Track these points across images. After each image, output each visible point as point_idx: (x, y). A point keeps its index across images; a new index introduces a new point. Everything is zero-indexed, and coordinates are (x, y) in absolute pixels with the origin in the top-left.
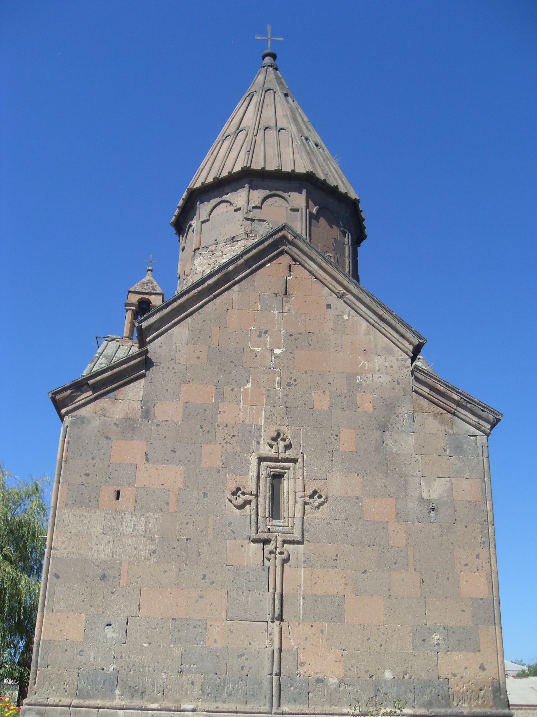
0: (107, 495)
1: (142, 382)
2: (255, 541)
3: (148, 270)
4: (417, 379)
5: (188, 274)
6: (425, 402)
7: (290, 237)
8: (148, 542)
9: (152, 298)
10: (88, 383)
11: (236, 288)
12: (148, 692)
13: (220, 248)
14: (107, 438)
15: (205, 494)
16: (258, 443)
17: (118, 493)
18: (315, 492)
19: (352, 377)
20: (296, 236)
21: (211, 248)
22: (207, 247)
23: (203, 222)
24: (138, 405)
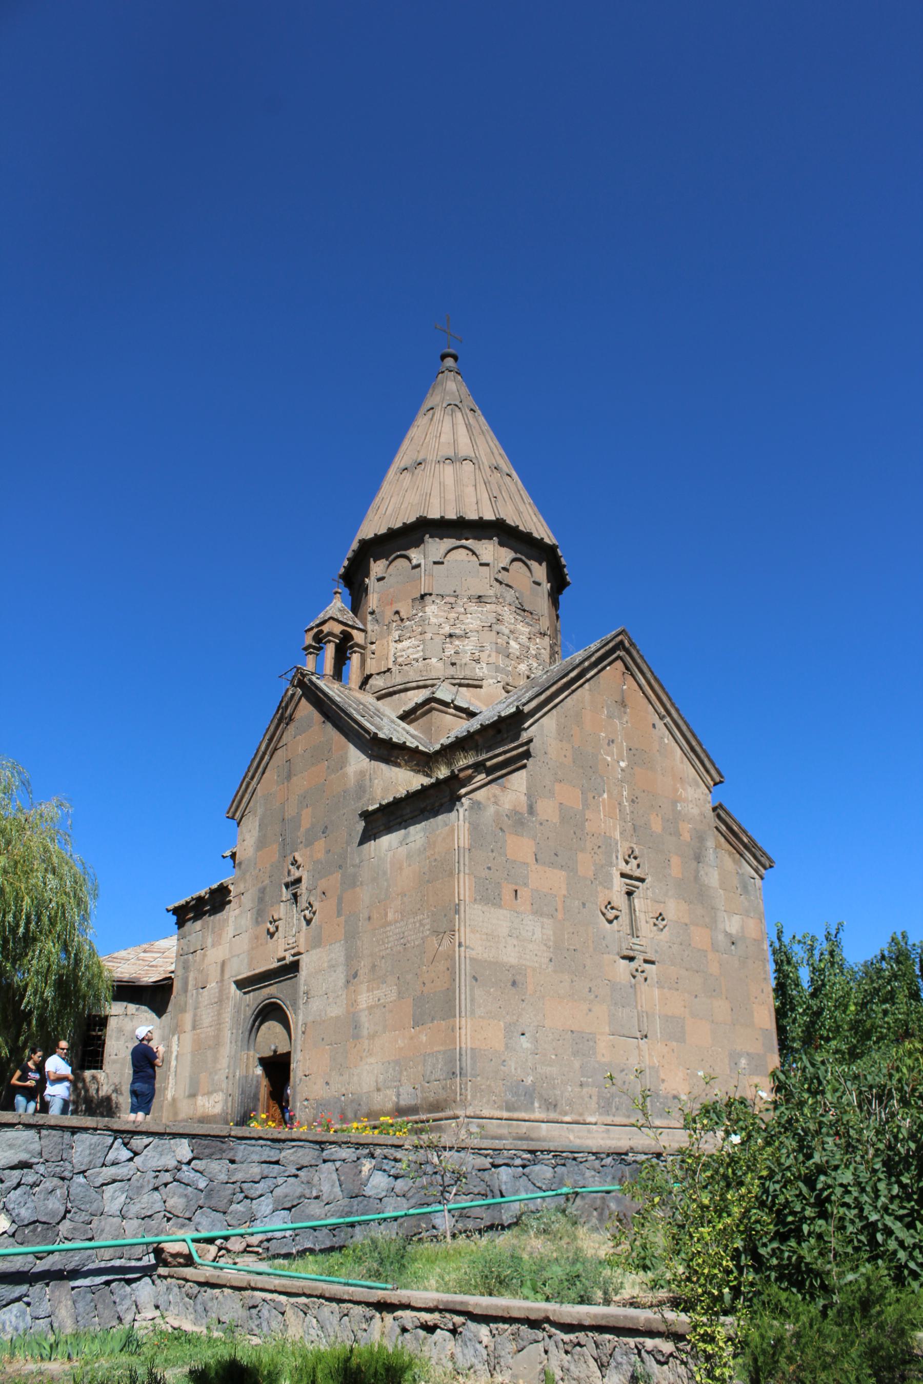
0: (507, 893)
1: (523, 773)
2: (624, 958)
3: (336, 593)
4: (719, 816)
6: (722, 840)
7: (627, 644)
8: (545, 948)
9: (355, 633)
10: (484, 765)
11: (587, 685)
12: (559, 1105)
14: (501, 829)
15: (584, 904)
16: (617, 857)
17: (516, 891)
18: (661, 914)
19: (674, 803)
20: (632, 644)
21: (448, 599)
23: (435, 563)
24: (523, 799)
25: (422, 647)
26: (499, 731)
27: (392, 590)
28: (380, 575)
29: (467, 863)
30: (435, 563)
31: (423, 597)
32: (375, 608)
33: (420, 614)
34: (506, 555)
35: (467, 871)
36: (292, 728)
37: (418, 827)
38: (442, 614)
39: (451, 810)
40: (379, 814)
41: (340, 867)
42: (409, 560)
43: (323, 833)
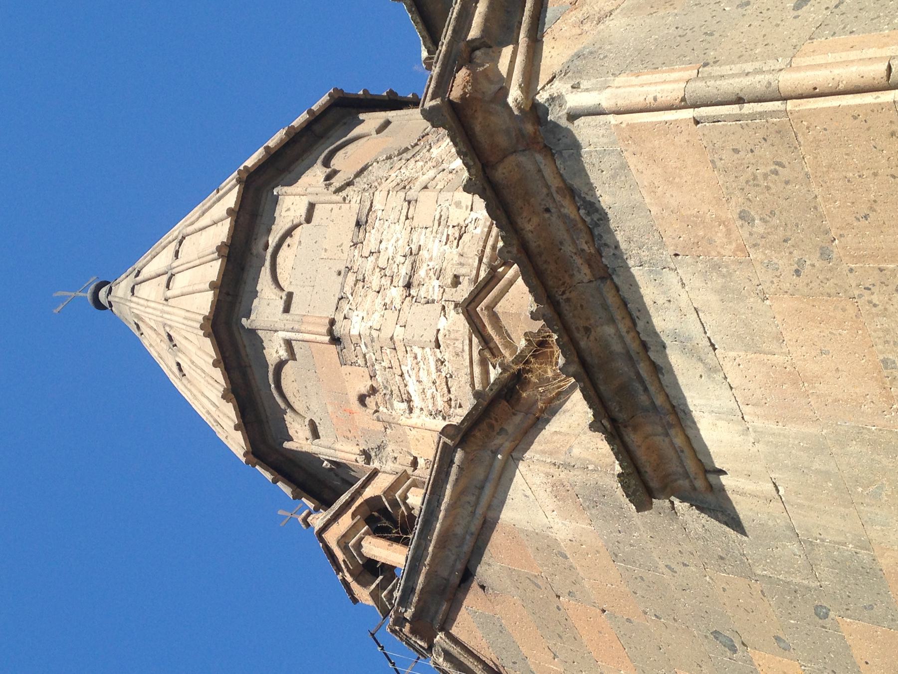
5: (369, 383)
9: (369, 493)
13: (360, 259)
21: (348, 289)
22: (342, 298)
23: (287, 310)
25: (416, 349)
27: (330, 409)
28: (308, 434)
29: (749, 67)
30: (287, 310)
31: (336, 340)
32: (357, 450)
33: (363, 346)
34: (315, 176)
35: (781, 63)
37: (649, 292)
38: (369, 298)
39: (575, 146)
40: (633, 438)
41: (821, 613)
42: (280, 365)
43: (734, 650)
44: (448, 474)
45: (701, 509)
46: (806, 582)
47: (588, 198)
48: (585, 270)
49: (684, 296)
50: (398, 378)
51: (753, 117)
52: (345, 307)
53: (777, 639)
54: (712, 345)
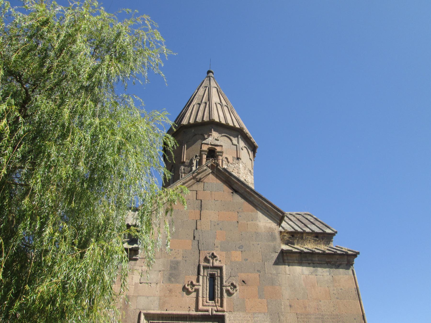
26: (317, 237)
28: (217, 138)
31: (238, 159)
36: (201, 185)
39: (348, 269)
40: (298, 255)
41: (258, 271)
44: (274, 208)
45: (278, 258)
46: (266, 271)
47: (340, 267)
48: (328, 261)
49: (325, 274)
50: (232, 170)
51: (357, 296)
52: (242, 163)
53: (247, 260)
54: (316, 275)
